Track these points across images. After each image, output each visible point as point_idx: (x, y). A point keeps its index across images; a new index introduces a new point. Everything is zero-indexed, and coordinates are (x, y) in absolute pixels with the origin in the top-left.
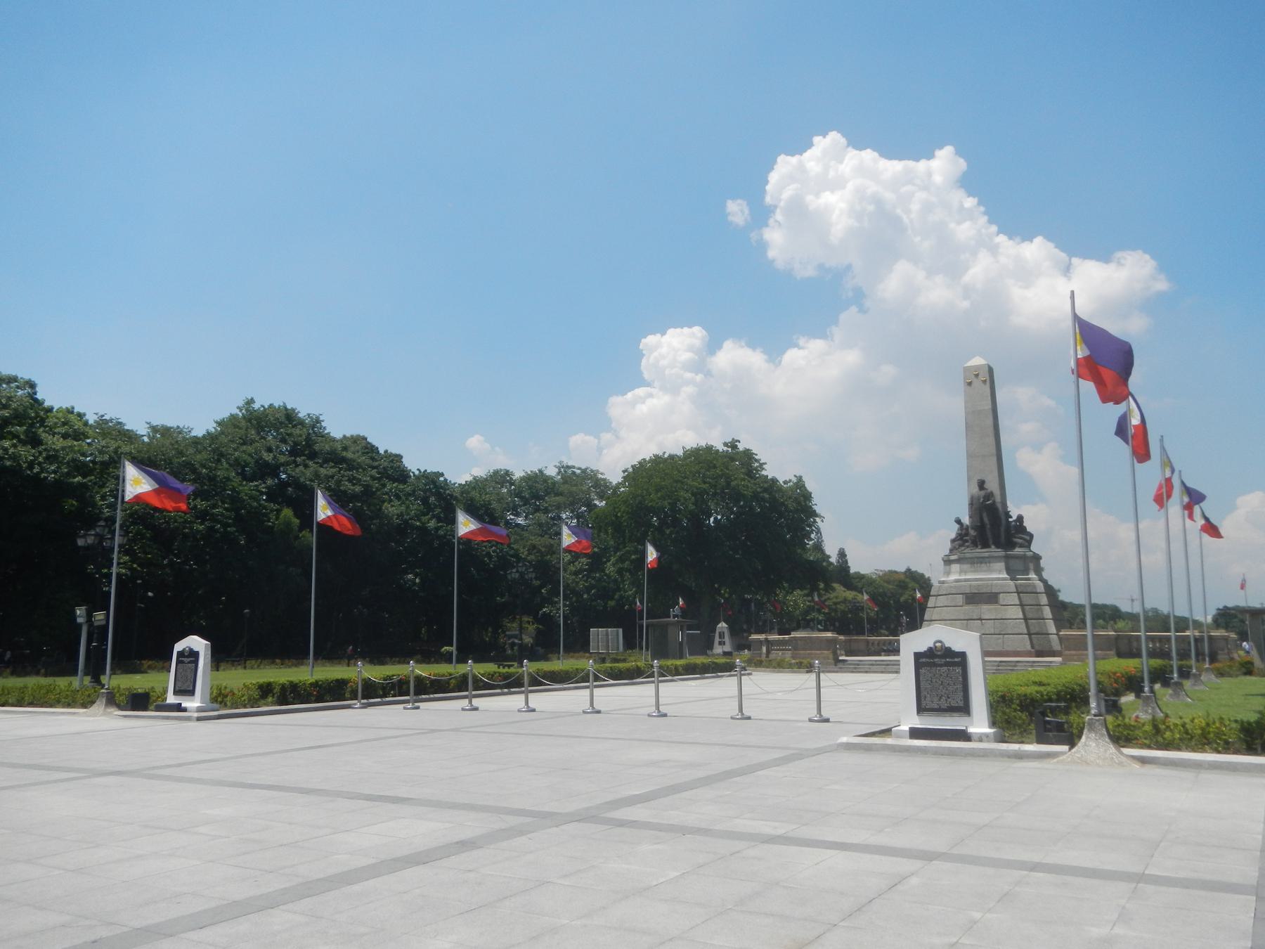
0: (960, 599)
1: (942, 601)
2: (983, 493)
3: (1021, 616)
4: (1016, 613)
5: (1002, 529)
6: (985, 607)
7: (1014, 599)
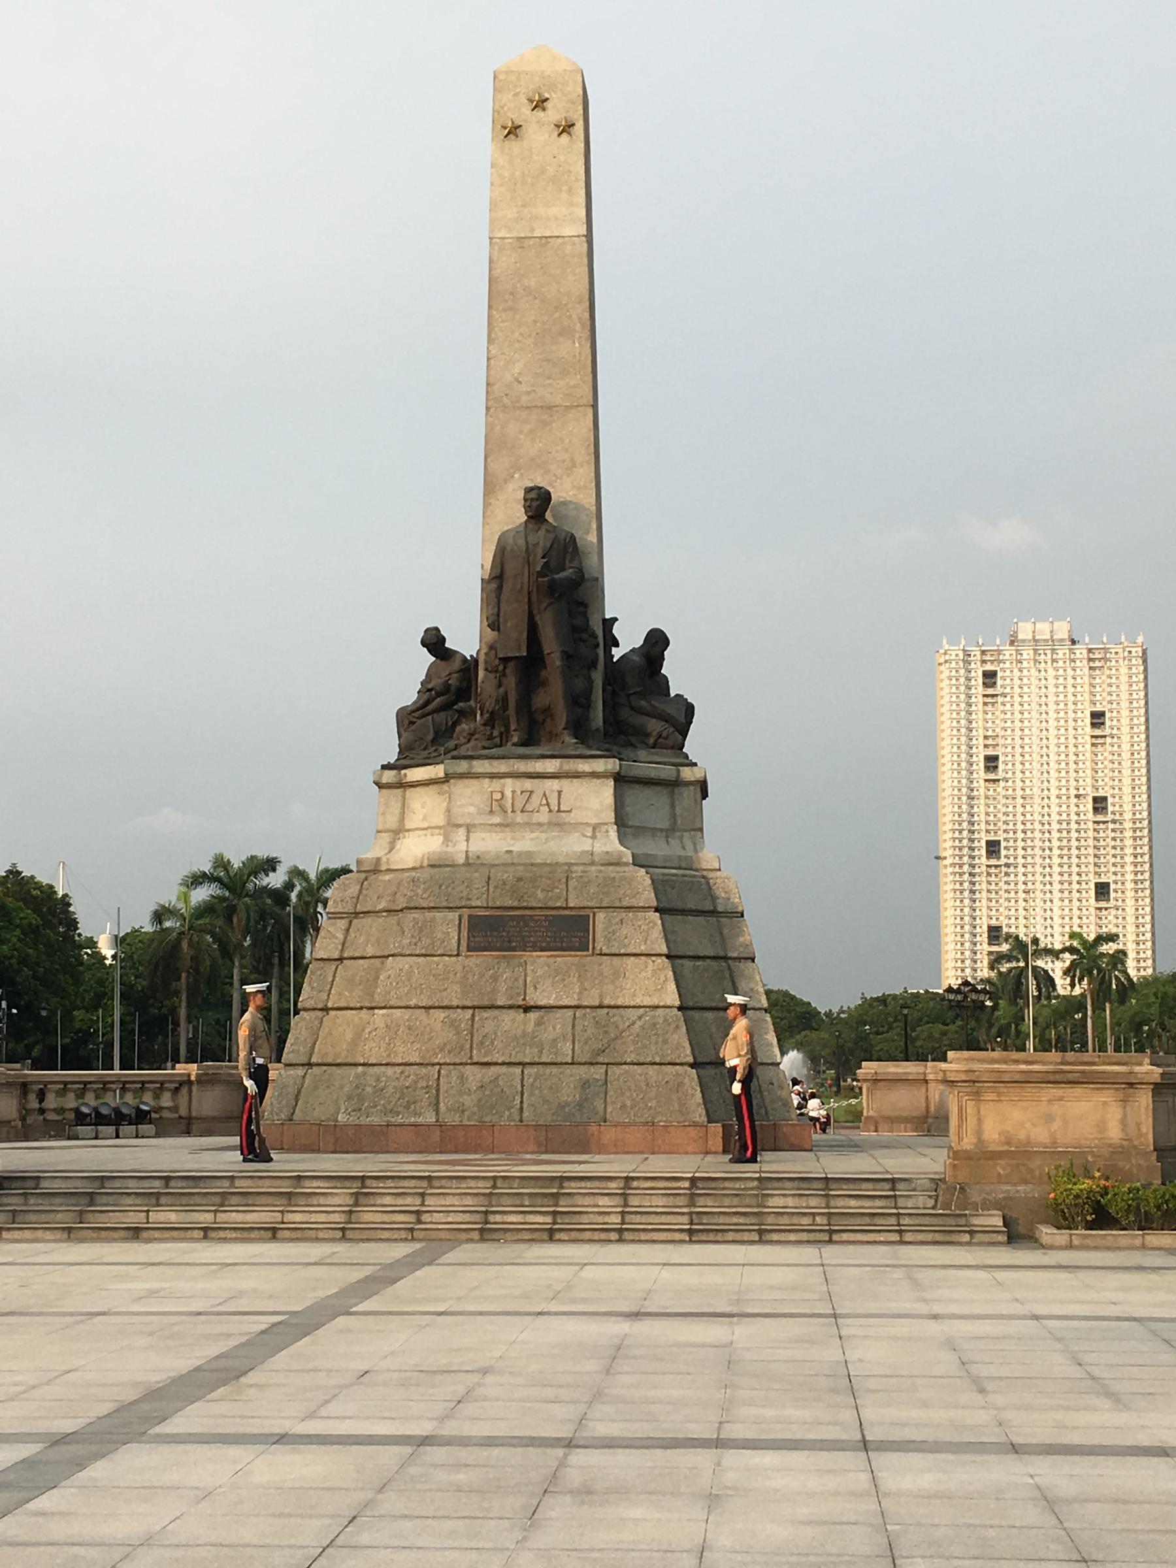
0: (448, 928)
1: (368, 936)
2: (541, 539)
3: (671, 996)
4: (651, 986)
5: (598, 676)
6: (539, 963)
7: (649, 932)
